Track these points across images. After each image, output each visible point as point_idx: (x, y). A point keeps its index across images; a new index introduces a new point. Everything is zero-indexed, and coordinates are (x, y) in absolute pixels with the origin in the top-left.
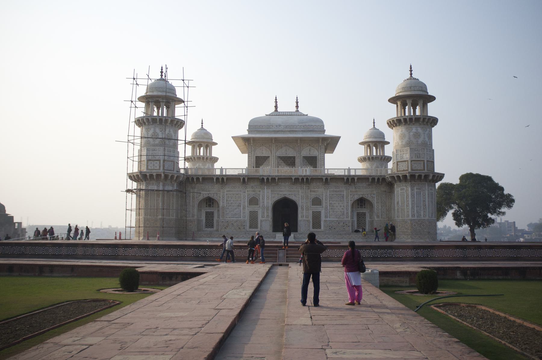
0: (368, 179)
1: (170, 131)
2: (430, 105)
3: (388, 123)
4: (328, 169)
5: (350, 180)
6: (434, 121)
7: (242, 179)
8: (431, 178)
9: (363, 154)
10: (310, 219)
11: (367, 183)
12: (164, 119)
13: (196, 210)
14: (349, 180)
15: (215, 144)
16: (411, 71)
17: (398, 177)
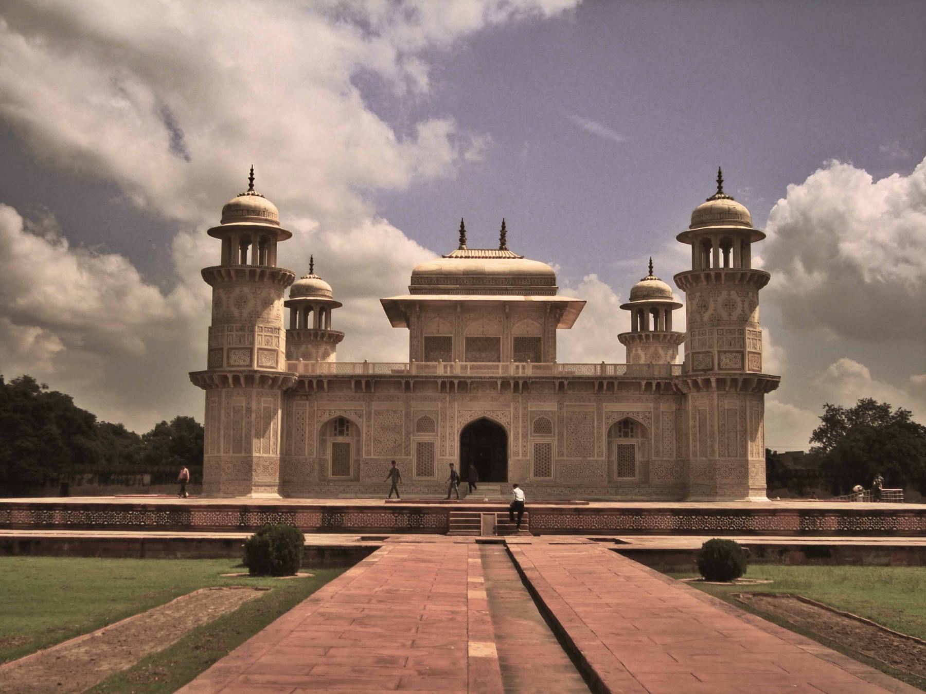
0: (639, 384)
1: (269, 294)
2: (756, 247)
3: (676, 281)
4: (564, 365)
5: (605, 387)
6: (761, 279)
7: (403, 382)
8: (754, 385)
9: (628, 329)
10: (531, 457)
11: (637, 392)
12: (258, 270)
13: (316, 444)
14: (601, 384)
15: (338, 305)
16: (720, 181)
17: (695, 383)
